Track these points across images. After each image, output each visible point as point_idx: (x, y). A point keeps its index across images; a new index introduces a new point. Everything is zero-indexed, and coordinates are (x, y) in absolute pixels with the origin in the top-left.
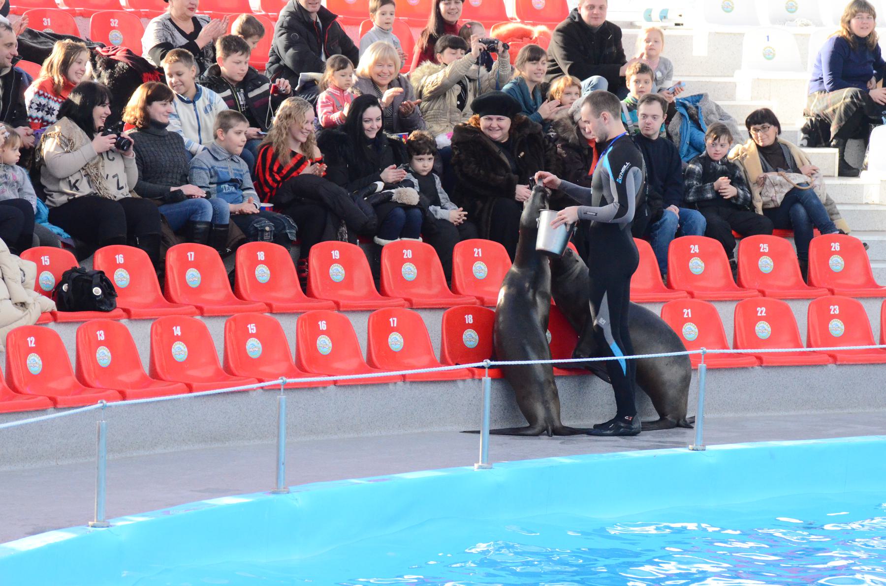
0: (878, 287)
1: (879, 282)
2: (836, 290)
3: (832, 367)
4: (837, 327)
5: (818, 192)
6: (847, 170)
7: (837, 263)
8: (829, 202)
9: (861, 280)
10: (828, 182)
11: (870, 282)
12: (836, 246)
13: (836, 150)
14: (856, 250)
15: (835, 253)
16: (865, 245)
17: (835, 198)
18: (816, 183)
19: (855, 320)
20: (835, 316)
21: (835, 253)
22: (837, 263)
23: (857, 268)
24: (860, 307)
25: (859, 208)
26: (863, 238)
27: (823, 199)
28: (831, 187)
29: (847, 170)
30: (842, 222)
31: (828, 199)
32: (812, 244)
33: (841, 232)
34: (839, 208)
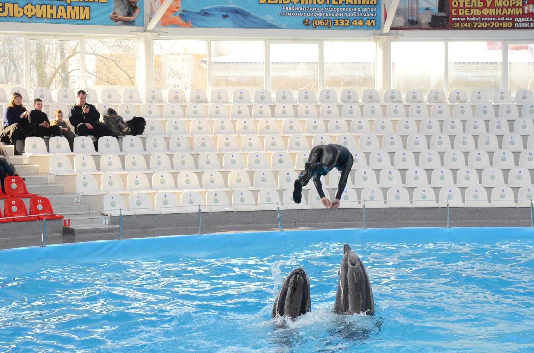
0: (28, 193)
1: (29, 192)
2: (14, 195)
3: (13, 223)
4: (14, 209)
5: (7, 161)
6: (17, 153)
7: (14, 186)
8: (12, 165)
9: (23, 192)
10: (11, 157)
11: (26, 192)
12: (14, 180)
13: (13, 146)
14: (21, 181)
15: (13, 182)
16: (24, 179)
17: (13, 163)
18: (7, 158)
19: (20, 206)
20: (13, 205)
21: (13, 182)
22: (14, 186)
23: (21, 188)
24: (22, 202)
25: (22, 166)
26: (22, 177)
27: (9, 164)
28: (11, 159)
29: (17, 153)
30: (17, 172)
31: (11, 164)
32: (5, 179)
33: (16, 175)
34: (15, 166)
